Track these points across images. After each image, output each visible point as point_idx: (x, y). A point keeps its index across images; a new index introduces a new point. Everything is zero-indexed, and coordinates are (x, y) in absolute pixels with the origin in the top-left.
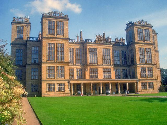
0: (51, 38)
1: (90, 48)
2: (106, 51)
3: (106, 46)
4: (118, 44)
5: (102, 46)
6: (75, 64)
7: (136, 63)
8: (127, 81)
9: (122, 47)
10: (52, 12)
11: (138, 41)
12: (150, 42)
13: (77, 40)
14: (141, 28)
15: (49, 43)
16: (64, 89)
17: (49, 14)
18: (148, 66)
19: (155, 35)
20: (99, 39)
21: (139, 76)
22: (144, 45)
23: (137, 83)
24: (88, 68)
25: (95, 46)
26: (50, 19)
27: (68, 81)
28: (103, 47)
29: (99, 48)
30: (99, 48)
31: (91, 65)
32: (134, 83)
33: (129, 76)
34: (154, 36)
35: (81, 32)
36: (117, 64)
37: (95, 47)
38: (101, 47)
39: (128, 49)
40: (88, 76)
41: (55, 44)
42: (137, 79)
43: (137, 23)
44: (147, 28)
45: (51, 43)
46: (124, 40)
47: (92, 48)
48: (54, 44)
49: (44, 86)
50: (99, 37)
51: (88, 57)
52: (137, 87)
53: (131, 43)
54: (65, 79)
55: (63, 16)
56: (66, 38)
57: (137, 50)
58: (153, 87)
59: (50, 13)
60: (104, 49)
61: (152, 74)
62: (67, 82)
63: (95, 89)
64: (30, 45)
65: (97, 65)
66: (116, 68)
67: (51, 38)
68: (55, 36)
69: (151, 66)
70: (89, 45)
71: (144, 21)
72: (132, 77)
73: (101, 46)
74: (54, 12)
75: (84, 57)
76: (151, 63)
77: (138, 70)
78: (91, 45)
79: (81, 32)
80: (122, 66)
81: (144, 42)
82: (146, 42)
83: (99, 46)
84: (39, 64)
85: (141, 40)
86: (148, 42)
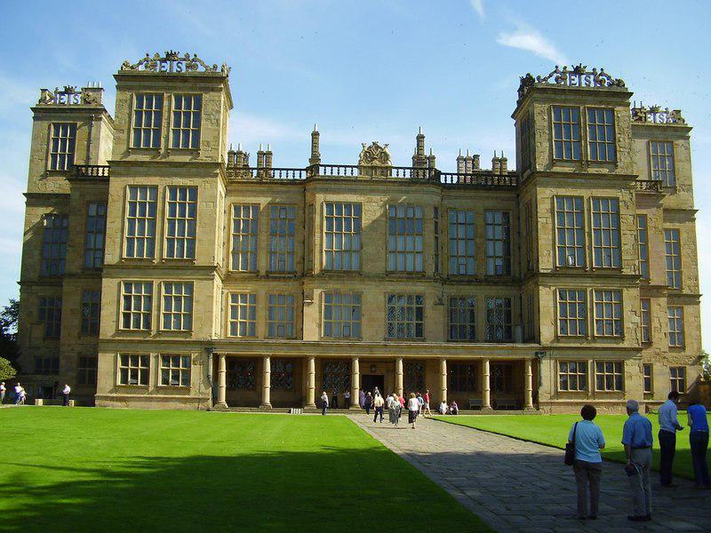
1: (329, 205)
4: (478, 182)
6: (263, 272)
7: (538, 267)
8: (487, 353)
9: (491, 194)
13: (458, 174)
15: (134, 188)
16: (187, 381)
17: (141, 68)
18: (599, 285)
20: (377, 163)
21: (547, 332)
23: (536, 363)
24: (317, 292)
27: (208, 347)
30: (370, 201)
32: (521, 364)
33: (518, 331)
35: (315, 135)
36: (462, 271)
39: (518, 204)
40: (312, 330)
41: (160, 190)
42: (537, 345)
43: (552, 81)
45: (144, 188)
46: (503, 161)
47: (339, 205)
48: (154, 188)
49: (108, 365)
50: (375, 157)
52: (537, 383)
53: (525, 175)
54: (193, 338)
55: (201, 69)
56: (209, 160)
57: (543, 208)
58: (621, 386)
59: (145, 60)
61: (620, 323)
62: (203, 347)
63: (370, 383)
64: (81, 195)
65: (359, 275)
66: (453, 290)
71: (587, 70)
72: (526, 336)
75: (304, 242)
77: (547, 298)
79: (315, 135)
80: (488, 281)
84: (96, 272)
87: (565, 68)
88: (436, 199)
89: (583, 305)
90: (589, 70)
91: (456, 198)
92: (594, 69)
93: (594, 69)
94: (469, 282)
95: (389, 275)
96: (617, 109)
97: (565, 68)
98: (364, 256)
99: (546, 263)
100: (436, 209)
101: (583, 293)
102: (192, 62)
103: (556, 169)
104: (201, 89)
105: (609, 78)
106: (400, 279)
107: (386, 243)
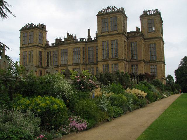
10: (27, 25)
11: (102, 33)
18: (112, 62)
20: (70, 39)
22: (108, 38)
26: (25, 32)
29: (69, 48)
30: (69, 48)
31: (62, 66)
37: (66, 48)
38: (72, 46)
44: (113, 15)
48: (26, 52)
60: (74, 48)
68: (28, 45)
69: (117, 62)
70: (61, 47)
74: (27, 25)
76: (116, 58)
81: (109, 33)
83: (70, 46)
85: (105, 32)
87: (105, 8)
88: (84, 45)
89: (108, 68)
90: (111, 7)
91: (89, 44)
92: (113, 7)
93: (113, 7)
94: (92, 64)
95: (73, 65)
96: (118, 16)
97: (105, 8)
98: (68, 61)
99: (100, 58)
100: (83, 48)
101: (108, 65)
102: (32, 25)
103: (102, 35)
104: (34, 30)
105: (116, 8)
106: (75, 65)
107: (73, 57)
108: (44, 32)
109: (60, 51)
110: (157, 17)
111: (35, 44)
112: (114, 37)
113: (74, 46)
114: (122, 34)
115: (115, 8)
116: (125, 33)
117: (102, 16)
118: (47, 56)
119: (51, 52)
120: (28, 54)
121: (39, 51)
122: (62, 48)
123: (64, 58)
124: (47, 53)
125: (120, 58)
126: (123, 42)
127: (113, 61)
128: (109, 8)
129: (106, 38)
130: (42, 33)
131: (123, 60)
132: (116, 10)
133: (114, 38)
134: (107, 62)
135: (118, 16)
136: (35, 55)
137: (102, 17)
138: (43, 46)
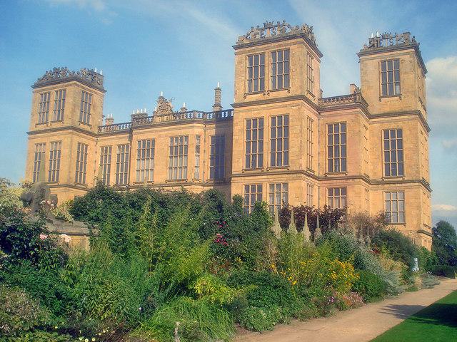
0: (40, 132)
2: (82, 151)
3: (180, 129)
5: (169, 130)
11: (245, 97)
12: (289, 91)
14: (259, 49)
18: (272, 179)
19: (404, 54)
20: (165, 112)
22: (264, 109)
25: (152, 132)
26: (44, 90)
28: (170, 132)
30: (160, 136)
34: (402, 57)
37: (151, 136)
44: (280, 46)
51: (135, 164)
67: (40, 132)
69: (283, 178)
73: (166, 130)
76: (283, 168)
78: (141, 133)
81: (267, 97)
82: (273, 95)
86: (283, 94)
96: (292, 47)
101: (260, 187)
102: (65, 70)
103: (246, 100)
104: (67, 86)
105: (289, 26)
108: (96, 93)
109: (135, 146)
110: (408, 53)
111: (67, 123)
112: (280, 107)
113: (174, 132)
114: (302, 97)
115: (287, 27)
116: (313, 96)
117: (247, 49)
118: (102, 157)
119: (111, 147)
120: (48, 150)
121: (79, 144)
122: (141, 137)
123: (144, 164)
124: (102, 149)
125: (292, 167)
126: (305, 123)
127: (274, 176)
128: (268, 26)
129: (258, 109)
130: (91, 95)
131: (301, 172)
132: (288, 30)
133: (278, 110)
134: (256, 177)
135: (292, 47)
136: (65, 151)
137: (249, 51)
138: (90, 130)
